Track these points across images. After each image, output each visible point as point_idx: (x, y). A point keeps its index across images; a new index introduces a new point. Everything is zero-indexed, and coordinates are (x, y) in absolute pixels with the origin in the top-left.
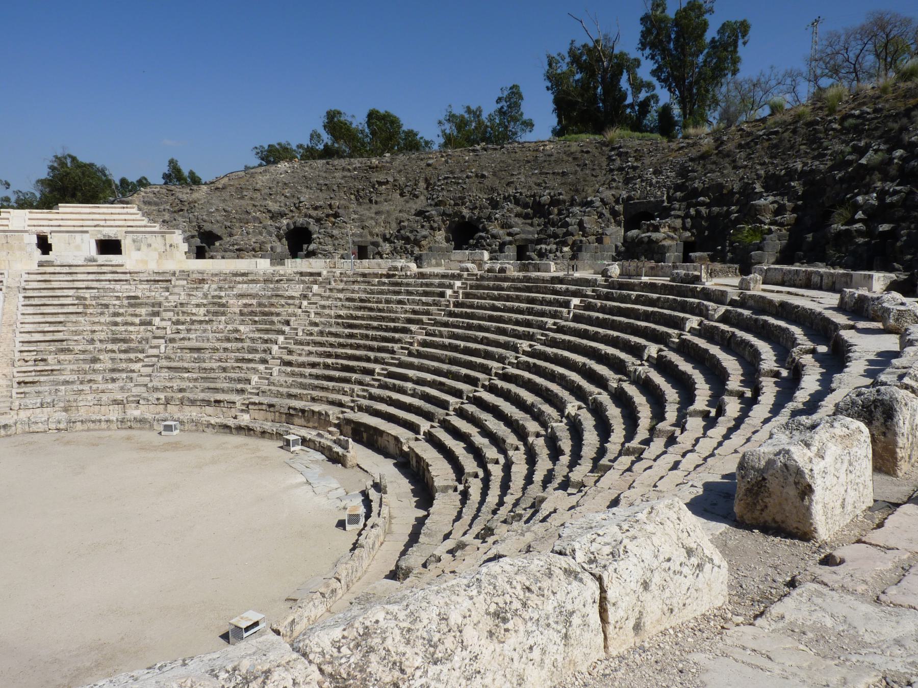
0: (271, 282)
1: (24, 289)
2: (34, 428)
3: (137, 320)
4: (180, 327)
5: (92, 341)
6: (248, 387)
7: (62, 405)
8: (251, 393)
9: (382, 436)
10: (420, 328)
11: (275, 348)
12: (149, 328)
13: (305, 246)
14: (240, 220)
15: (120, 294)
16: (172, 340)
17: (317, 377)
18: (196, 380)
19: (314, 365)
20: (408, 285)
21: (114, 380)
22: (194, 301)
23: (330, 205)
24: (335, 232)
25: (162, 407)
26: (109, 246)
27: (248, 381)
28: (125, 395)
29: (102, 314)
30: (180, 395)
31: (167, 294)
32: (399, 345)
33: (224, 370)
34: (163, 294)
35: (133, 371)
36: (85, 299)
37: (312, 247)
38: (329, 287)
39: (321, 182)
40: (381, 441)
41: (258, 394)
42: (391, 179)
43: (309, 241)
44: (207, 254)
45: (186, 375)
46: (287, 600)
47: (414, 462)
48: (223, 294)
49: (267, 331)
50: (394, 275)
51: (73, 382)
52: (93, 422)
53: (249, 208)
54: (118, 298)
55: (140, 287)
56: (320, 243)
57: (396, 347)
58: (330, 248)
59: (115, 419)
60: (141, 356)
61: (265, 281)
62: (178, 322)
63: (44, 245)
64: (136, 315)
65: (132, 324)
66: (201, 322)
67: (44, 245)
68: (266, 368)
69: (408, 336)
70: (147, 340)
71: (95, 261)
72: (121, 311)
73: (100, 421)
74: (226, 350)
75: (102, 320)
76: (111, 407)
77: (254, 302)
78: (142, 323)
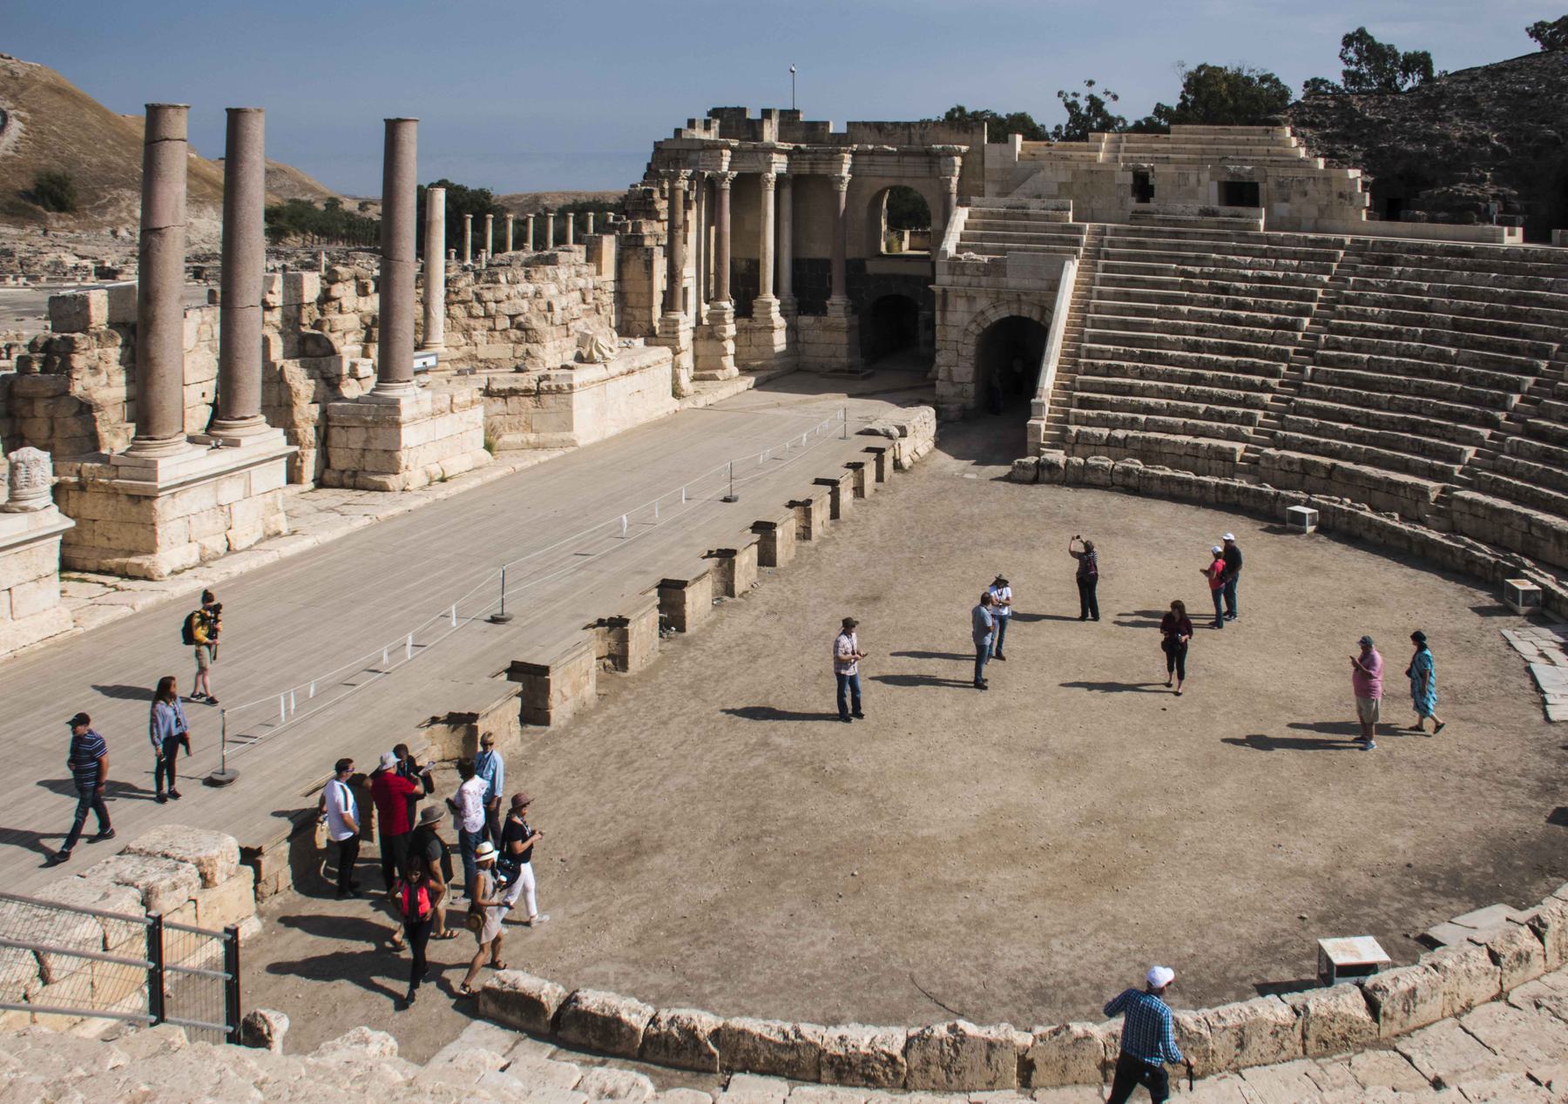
2: (1091, 477)
4: (1342, 338)
5: (1195, 347)
7: (1138, 446)
15: (1249, 273)
16: (1326, 361)
18: (1359, 438)
21: (1223, 417)
26: (1240, 193)
27: (1455, 457)
28: (1239, 447)
29: (1216, 303)
30: (1326, 461)
31: (1326, 278)
33: (1414, 427)
35: (1256, 407)
36: (1193, 275)
45: (1344, 426)
48: (1425, 286)
52: (1181, 482)
54: (1245, 279)
55: (1282, 261)
60: (1274, 382)
62: (1342, 330)
63: (1143, 187)
64: (1270, 311)
66: (1379, 334)
67: (1143, 187)
68: (1492, 437)
70: (1282, 356)
71: (1214, 213)
72: (1250, 300)
73: (1189, 482)
74: (1421, 391)
75: (1217, 311)
76: (1213, 464)
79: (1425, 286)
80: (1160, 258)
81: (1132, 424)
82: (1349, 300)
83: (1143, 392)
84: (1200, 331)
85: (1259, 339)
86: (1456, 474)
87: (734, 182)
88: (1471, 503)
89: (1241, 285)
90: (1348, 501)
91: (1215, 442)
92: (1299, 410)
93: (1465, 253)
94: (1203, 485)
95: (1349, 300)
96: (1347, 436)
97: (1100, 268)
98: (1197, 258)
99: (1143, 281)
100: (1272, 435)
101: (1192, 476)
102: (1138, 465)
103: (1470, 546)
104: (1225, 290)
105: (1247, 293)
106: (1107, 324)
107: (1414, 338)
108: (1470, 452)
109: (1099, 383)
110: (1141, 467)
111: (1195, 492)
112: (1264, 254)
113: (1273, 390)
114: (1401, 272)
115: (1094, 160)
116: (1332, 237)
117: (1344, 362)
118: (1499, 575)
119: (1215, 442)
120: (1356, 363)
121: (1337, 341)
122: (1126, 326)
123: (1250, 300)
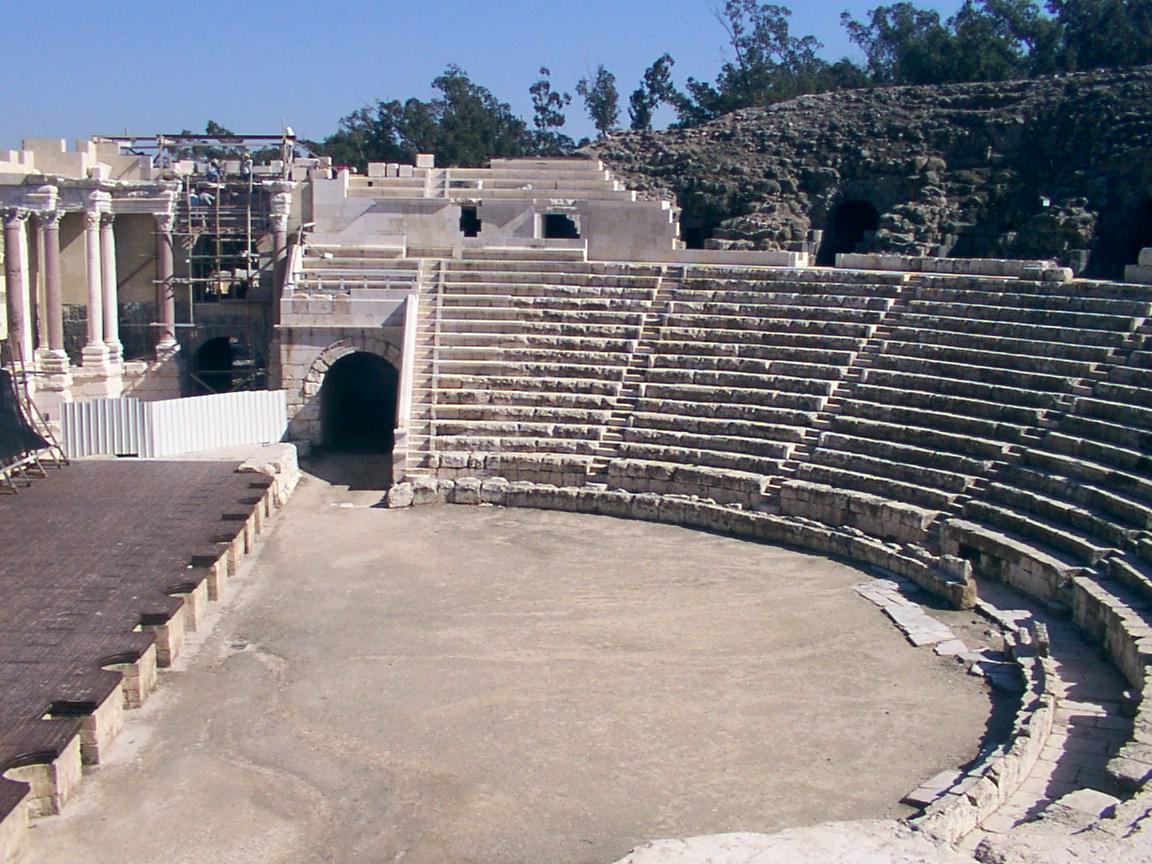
0: (816, 290)
1: (445, 290)
3: (602, 342)
6: (780, 462)
8: (784, 473)
9: (1017, 562)
10: (1082, 383)
11: (824, 400)
12: (622, 355)
13: (867, 234)
14: (760, 187)
15: (578, 301)
16: (657, 378)
17: (897, 455)
19: (889, 434)
20: (1057, 305)
21: (569, 434)
22: (687, 317)
23: (911, 166)
24: (921, 209)
25: (641, 483)
27: (780, 453)
28: (590, 459)
29: (552, 331)
30: (670, 466)
32: (1045, 411)
34: (643, 302)
35: (598, 422)
36: (526, 305)
37: (884, 232)
38: (914, 302)
39: (898, 124)
40: (1016, 573)
41: (793, 476)
42: (1020, 120)
43: (875, 225)
44: (706, 244)
45: (679, 434)
46: (906, 801)
47: (1081, 612)
48: (736, 307)
49: (810, 373)
50: (1031, 289)
51: (512, 433)
52: (547, 494)
53: (776, 168)
54: (574, 306)
55: (607, 289)
56: (894, 228)
57: (1040, 412)
58: (910, 238)
59: (575, 494)
60: (612, 400)
61: (803, 290)
62: (666, 349)
64: (601, 335)
65: (596, 348)
67: (470, 223)
68: (807, 433)
69: (1062, 395)
70: (618, 376)
72: (582, 326)
74: (741, 399)
75: (553, 338)
76: (566, 476)
77: (787, 321)
78: (610, 348)
79: (736, 307)
80: (496, 291)
81: (489, 446)
82: (672, 323)
83: (494, 415)
84: (539, 358)
85: (594, 361)
86: (781, 467)
87: (62, 222)
88: (798, 489)
89: (573, 313)
90: (696, 497)
91: (567, 457)
92: (639, 423)
93: (769, 276)
94: (565, 495)
95: (672, 323)
96: (683, 442)
97: (440, 302)
98: (530, 289)
99: (482, 313)
100: (617, 447)
101: (557, 490)
102: (502, 482)
103: (806, 524)
104: (558, 318)
105: (581, 320)
106: (454, 356)
107: (730, 353)
108: (791, 448)
109: (454, 411)
110: (507, 484)
111: (557, 502)
112: (589, 283)
113: (613, 408)
114: (714, 295)
115: (422, 194)
116: (650, 265)
117: (674, 378)
118: (834, 544)
119: (567, 457)
120: (683, 379)
121: (664, 359)
122: (472, 356)
123: (582, 326)
